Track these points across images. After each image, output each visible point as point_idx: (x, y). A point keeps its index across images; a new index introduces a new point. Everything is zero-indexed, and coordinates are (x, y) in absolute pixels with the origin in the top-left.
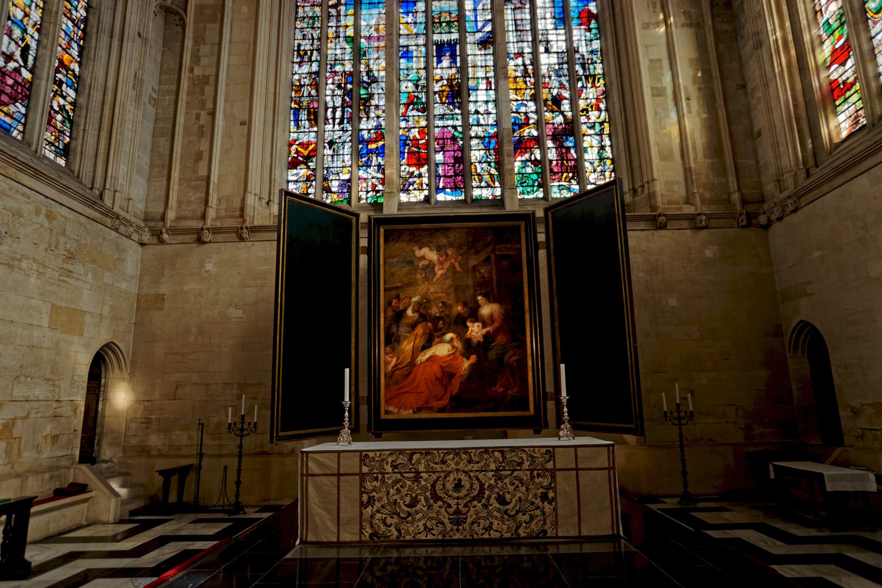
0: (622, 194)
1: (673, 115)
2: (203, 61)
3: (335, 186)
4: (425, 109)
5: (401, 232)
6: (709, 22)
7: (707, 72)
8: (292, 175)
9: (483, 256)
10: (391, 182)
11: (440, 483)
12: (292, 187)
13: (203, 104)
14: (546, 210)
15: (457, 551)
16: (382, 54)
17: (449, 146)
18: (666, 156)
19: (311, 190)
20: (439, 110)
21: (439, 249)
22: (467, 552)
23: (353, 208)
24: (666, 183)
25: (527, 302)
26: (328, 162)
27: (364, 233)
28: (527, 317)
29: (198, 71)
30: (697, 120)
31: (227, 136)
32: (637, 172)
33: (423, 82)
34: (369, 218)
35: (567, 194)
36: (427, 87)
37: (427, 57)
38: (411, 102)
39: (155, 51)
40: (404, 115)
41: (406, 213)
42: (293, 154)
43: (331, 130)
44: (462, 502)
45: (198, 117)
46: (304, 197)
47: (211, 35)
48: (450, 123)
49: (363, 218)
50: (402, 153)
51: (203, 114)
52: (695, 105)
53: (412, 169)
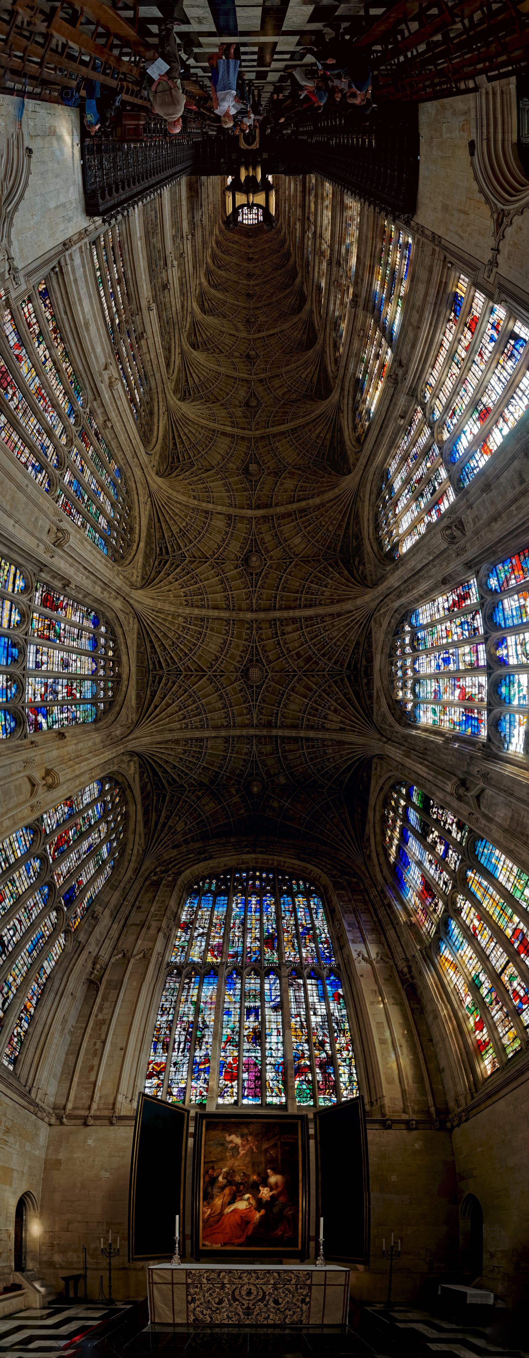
0: (364, 1105)
1: (393, 1056)
2: (105, 1011)
3: (175, 1091)
4: (238, 1045)
5: (217, 1123)
6: (407, 1003)
7: (410, 1031)
8: (148, 1083)
9: (272, 1143)
10: (212, 1091)
11: (237, 1291)
12: (147, 1091)
13: (99, 1037)
14: (315, 1114)
15: (247, 1330)
16: (213, 1012)
17: (252, 1068)
18: (391, 1081)
19: (159, 1094)
20: (246, 1046)
21: (242, 1136)
22: (253, 1331)
23: (186, 1107)
24: (391, 1099)
25: (300, 1175)
26: (172, 1076)
27: (192, 1124)
28: (300, 1185)
29: (100, 1017)
30: (407, 1060)
31: (111, 1056)
32: (373, 1090)
33: (237, 1029)
34: (196, 1113)
35: (329, 1104)
36: (239, 1033)
37: (240, 1015)
38: (229, 1041)
39: (78, 1004)
40: (224, 1048)
41: (221, 1111)
42: (150, 1070)
43: (176, 1056)
44: (251, 1303)
45: (95, 1044)
46: (154, 1097)
47: (112, 997)
48: (253, 1054)
49: (192, 1113)
50: (221, 1072)
51: (99, 1042)
52: (405, 1050)
53: (227, 1083)
